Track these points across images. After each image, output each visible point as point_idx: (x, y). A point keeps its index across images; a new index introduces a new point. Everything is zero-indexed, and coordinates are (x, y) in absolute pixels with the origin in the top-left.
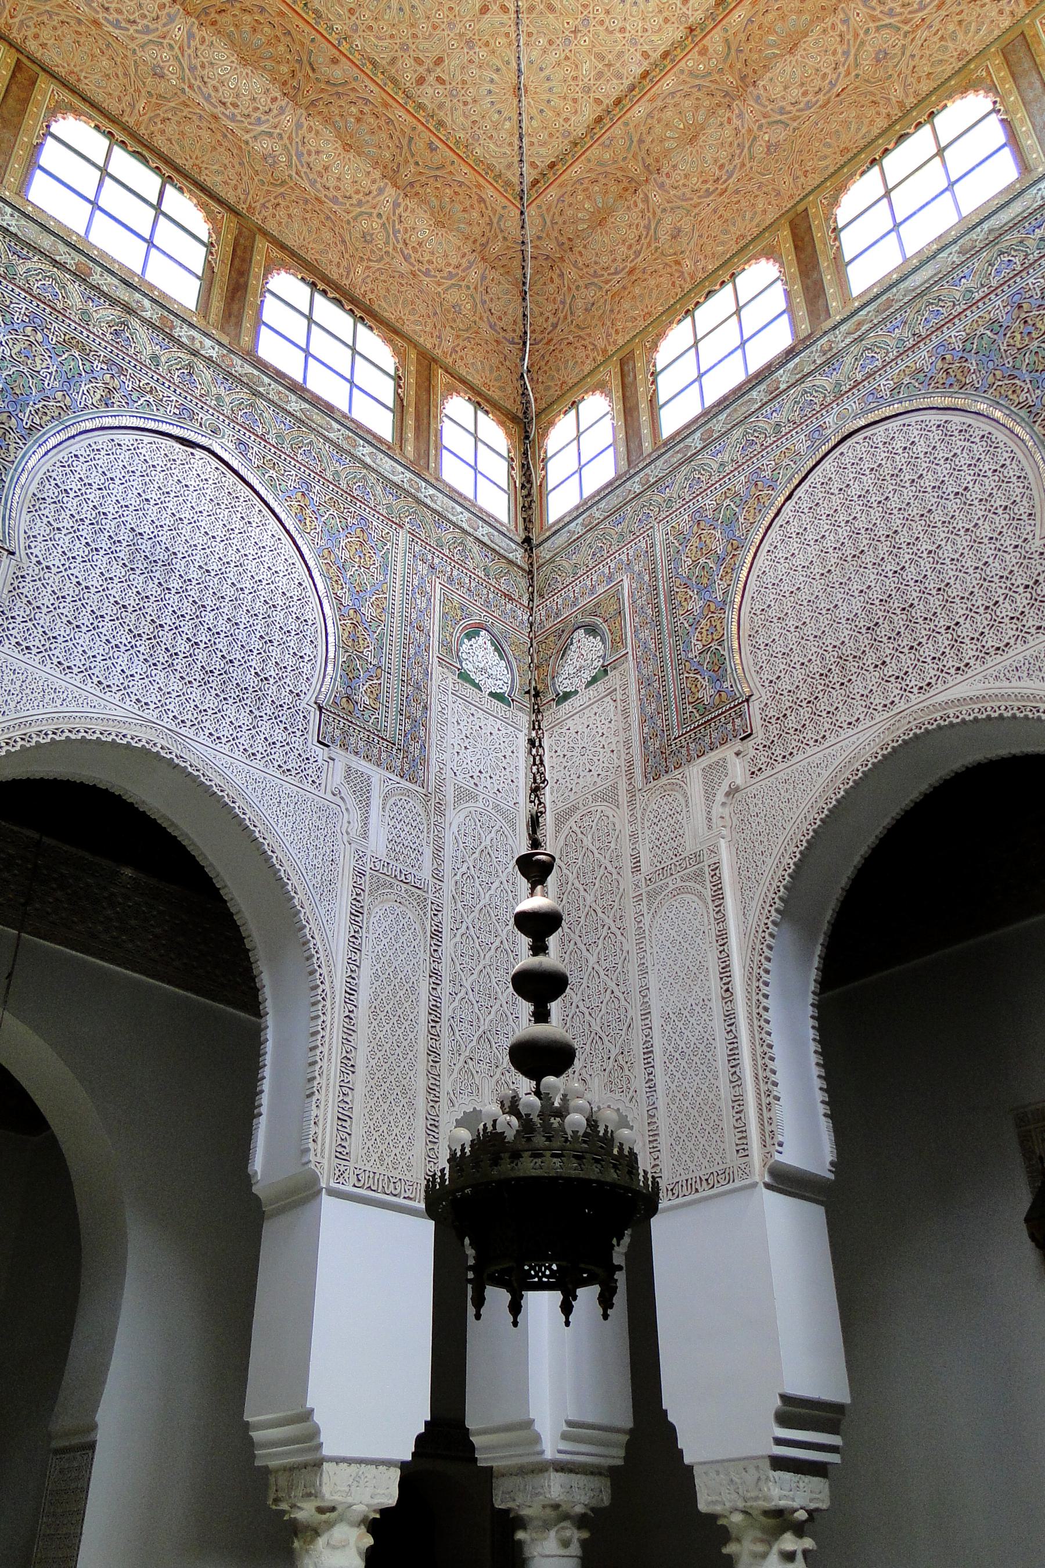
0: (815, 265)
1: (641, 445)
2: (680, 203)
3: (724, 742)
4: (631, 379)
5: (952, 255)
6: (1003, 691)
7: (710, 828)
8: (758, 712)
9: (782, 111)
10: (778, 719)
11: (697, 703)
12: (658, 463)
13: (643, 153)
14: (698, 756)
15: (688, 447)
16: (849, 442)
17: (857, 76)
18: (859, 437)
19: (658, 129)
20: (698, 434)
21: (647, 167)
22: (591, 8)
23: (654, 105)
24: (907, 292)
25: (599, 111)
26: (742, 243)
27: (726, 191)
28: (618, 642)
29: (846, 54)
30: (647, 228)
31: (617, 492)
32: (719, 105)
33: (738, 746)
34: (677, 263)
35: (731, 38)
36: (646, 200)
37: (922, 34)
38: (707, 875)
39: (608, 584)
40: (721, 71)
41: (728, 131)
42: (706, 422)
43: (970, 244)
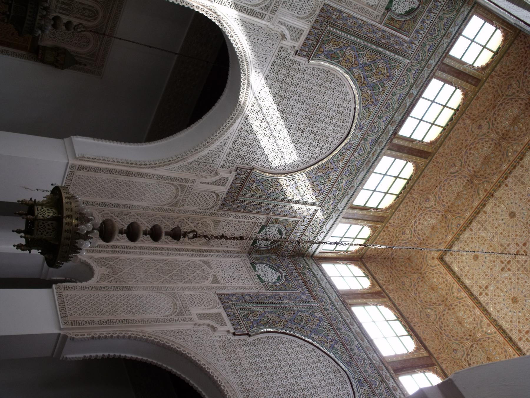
0: (408, 153)
1: (444, 71)
2: (482, 137)
3: (304, 44)
4: (470, 80)
5: (356, 183)
6: (222, 137)
7: (279, 22)
8: (300, 61)
9: (455, 176)
10: (290, 66)
11: (329, 42)
12: (428, 74)
13: (502, 150)
14: (310, 31)
15: (417, 87)
16: (346, 133)
17: (433, 193)
18: (343, 137)
19: (498, 160)
20: (415, 93)
21: (500, 145)
22: (527, 200)
23: (500, 170)
24: (363, 170)
25: (522, 162)
26: (448, 138)
27: (465, 147)
28: (391, 22)
29: (439, 198)
30: (493, 124)
31: (441, 54)
32: (478, 172)
33: (296, 48)
34: (474, 120)
35: (478, 196)
36: (497, 133)
37: (417, 209)
38: (263, 12)
39: (417, 29)
40: (479, 184)
41: (472, 165)
42: (415, 98)
43: (351, 189)
